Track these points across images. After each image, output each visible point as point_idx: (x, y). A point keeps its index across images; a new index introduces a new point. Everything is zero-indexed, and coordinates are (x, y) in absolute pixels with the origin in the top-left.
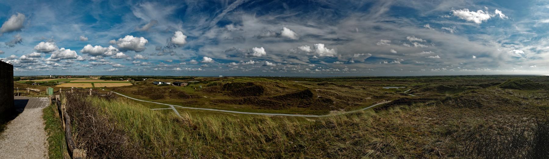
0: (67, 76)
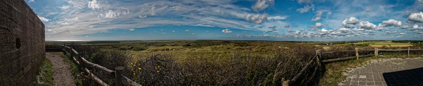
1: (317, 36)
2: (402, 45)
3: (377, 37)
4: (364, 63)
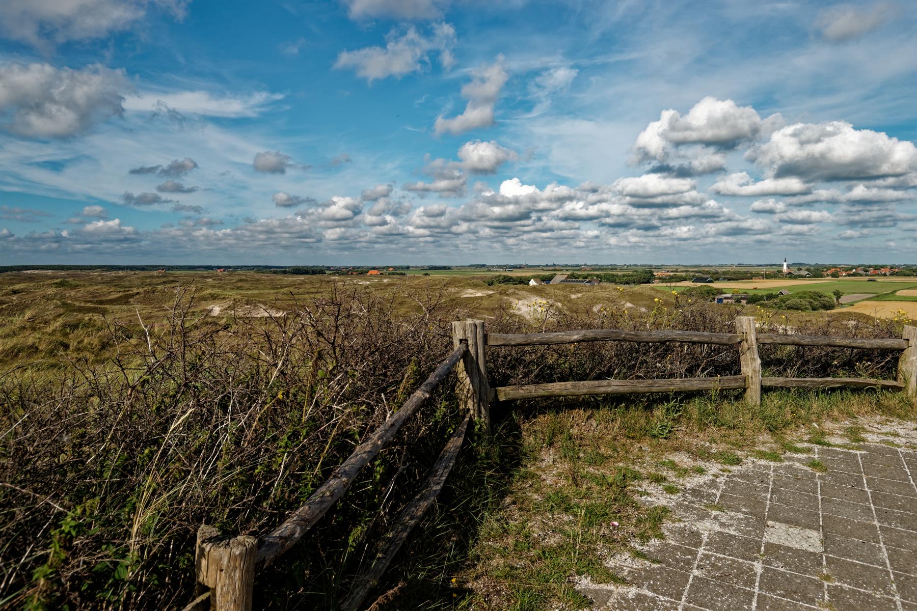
0: (870, 266)
1: (470, 231)
4: (806, 438)
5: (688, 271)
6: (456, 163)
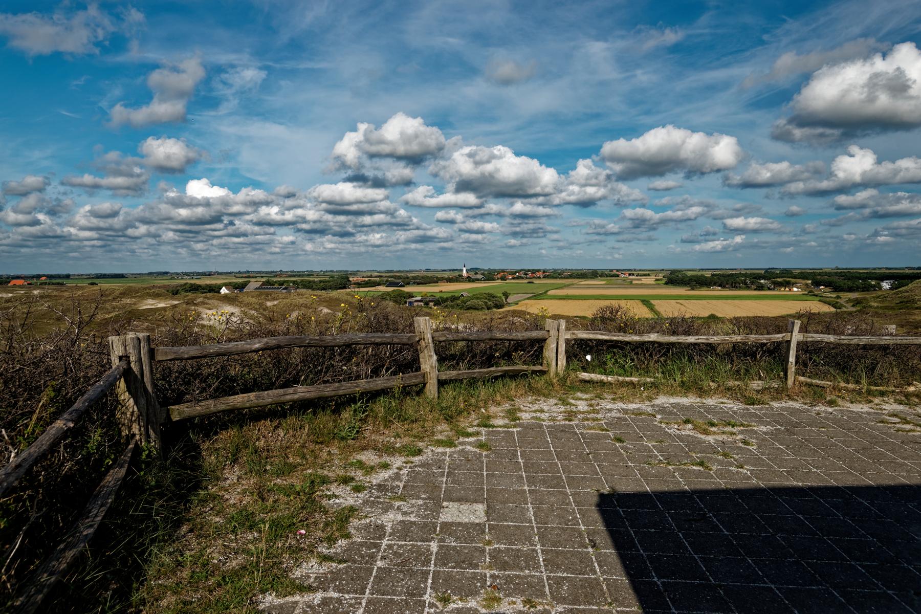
0: (529, 270)
1: (149, 235)
2: (737, 302)
3: (560, 248)
4: (476, 423)
5: (382, 277)
6: (136, 159)
